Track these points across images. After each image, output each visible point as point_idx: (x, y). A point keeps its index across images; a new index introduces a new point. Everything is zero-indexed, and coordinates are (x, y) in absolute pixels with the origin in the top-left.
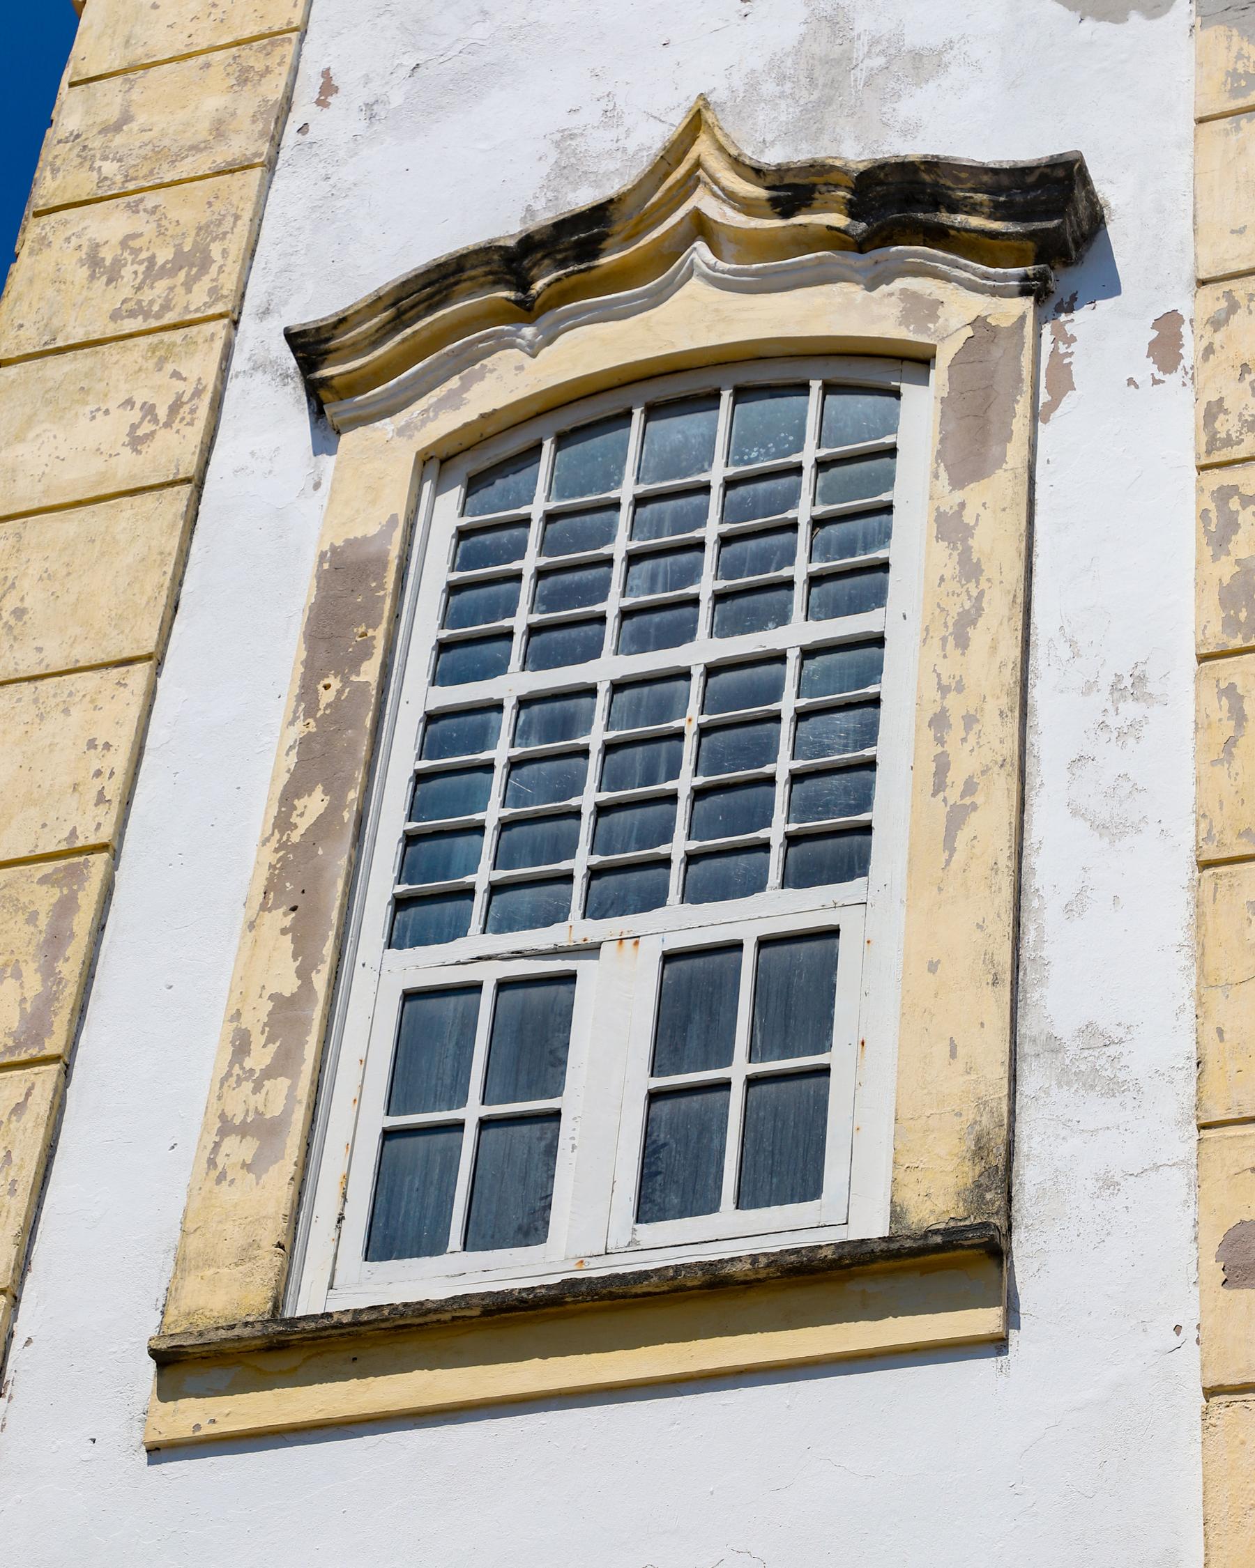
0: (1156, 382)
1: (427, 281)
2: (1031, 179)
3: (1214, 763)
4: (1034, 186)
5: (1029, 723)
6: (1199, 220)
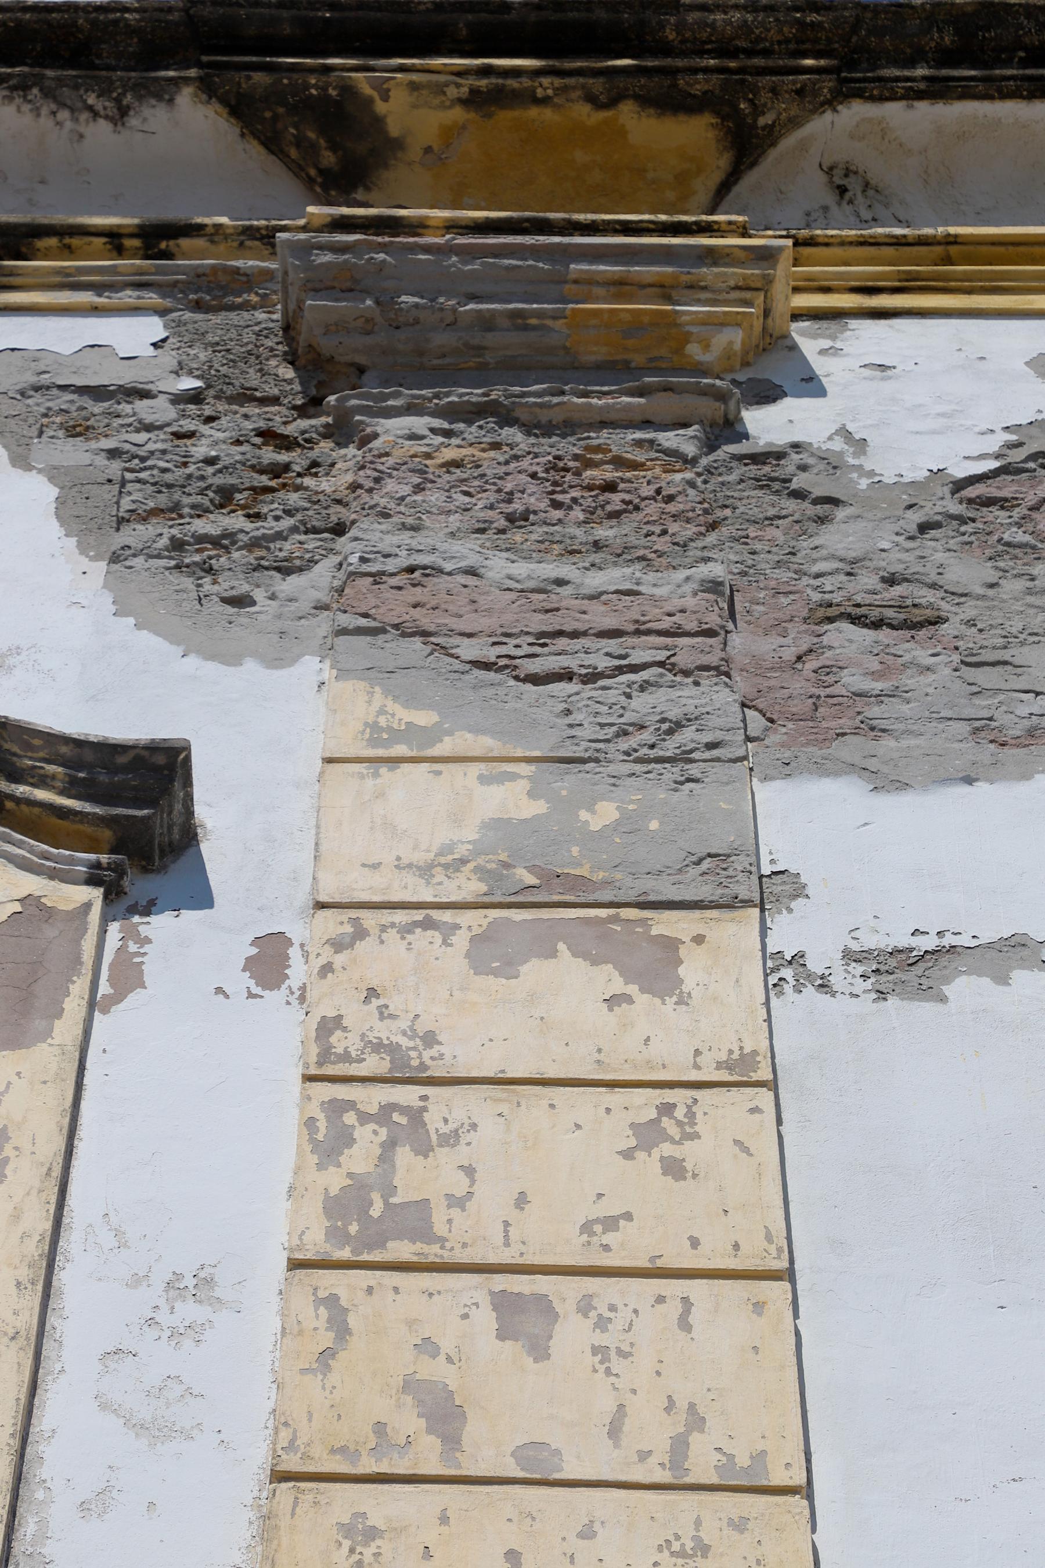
0: (251, 995)
2: (122, 760)
3: (303, 1371)
4: (125, 769)
5: (52, 1304)
6: (323, 848)
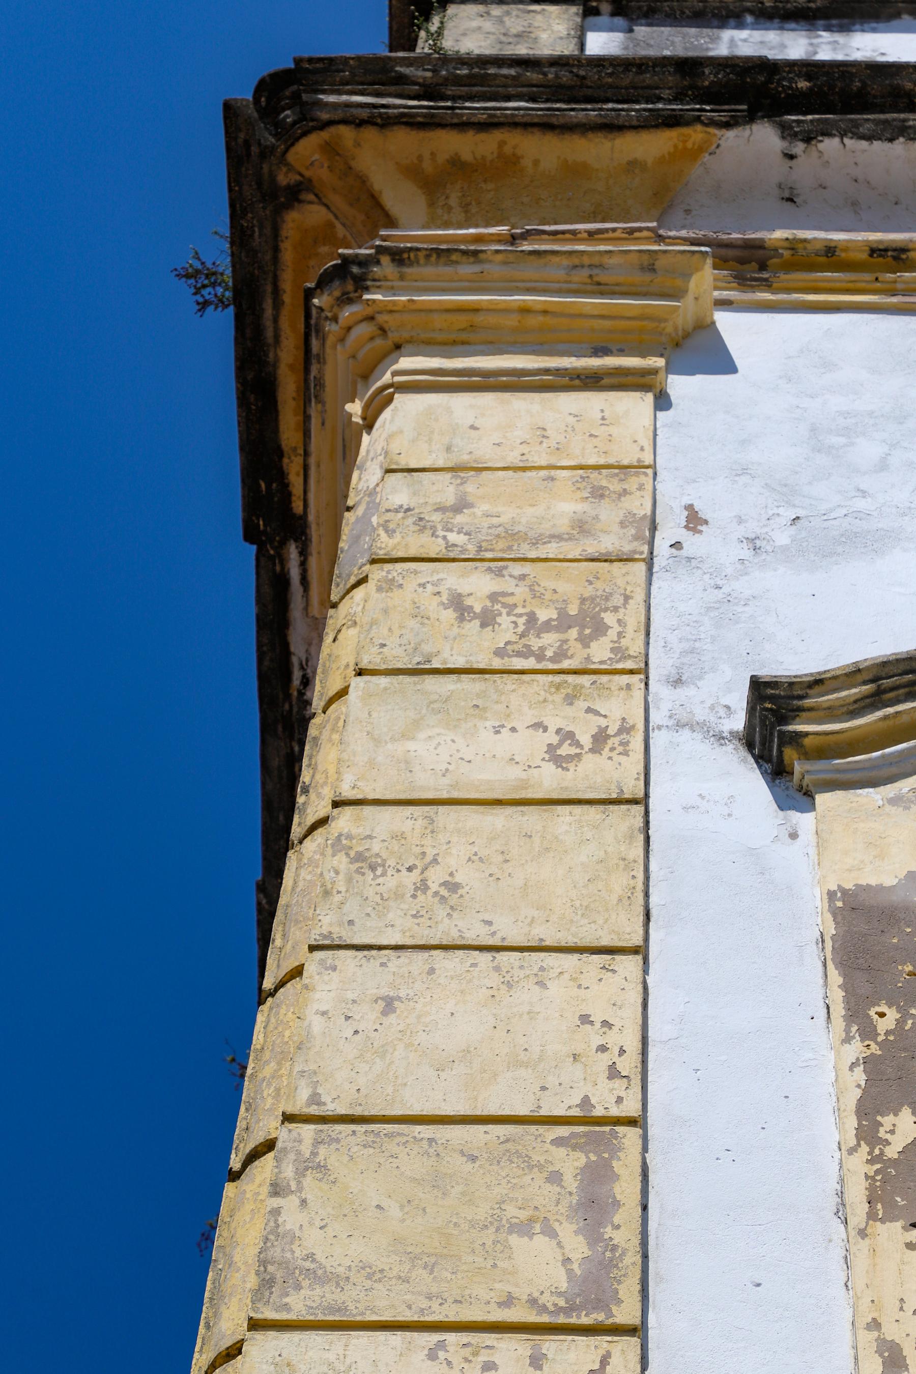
1: (908, 668)
